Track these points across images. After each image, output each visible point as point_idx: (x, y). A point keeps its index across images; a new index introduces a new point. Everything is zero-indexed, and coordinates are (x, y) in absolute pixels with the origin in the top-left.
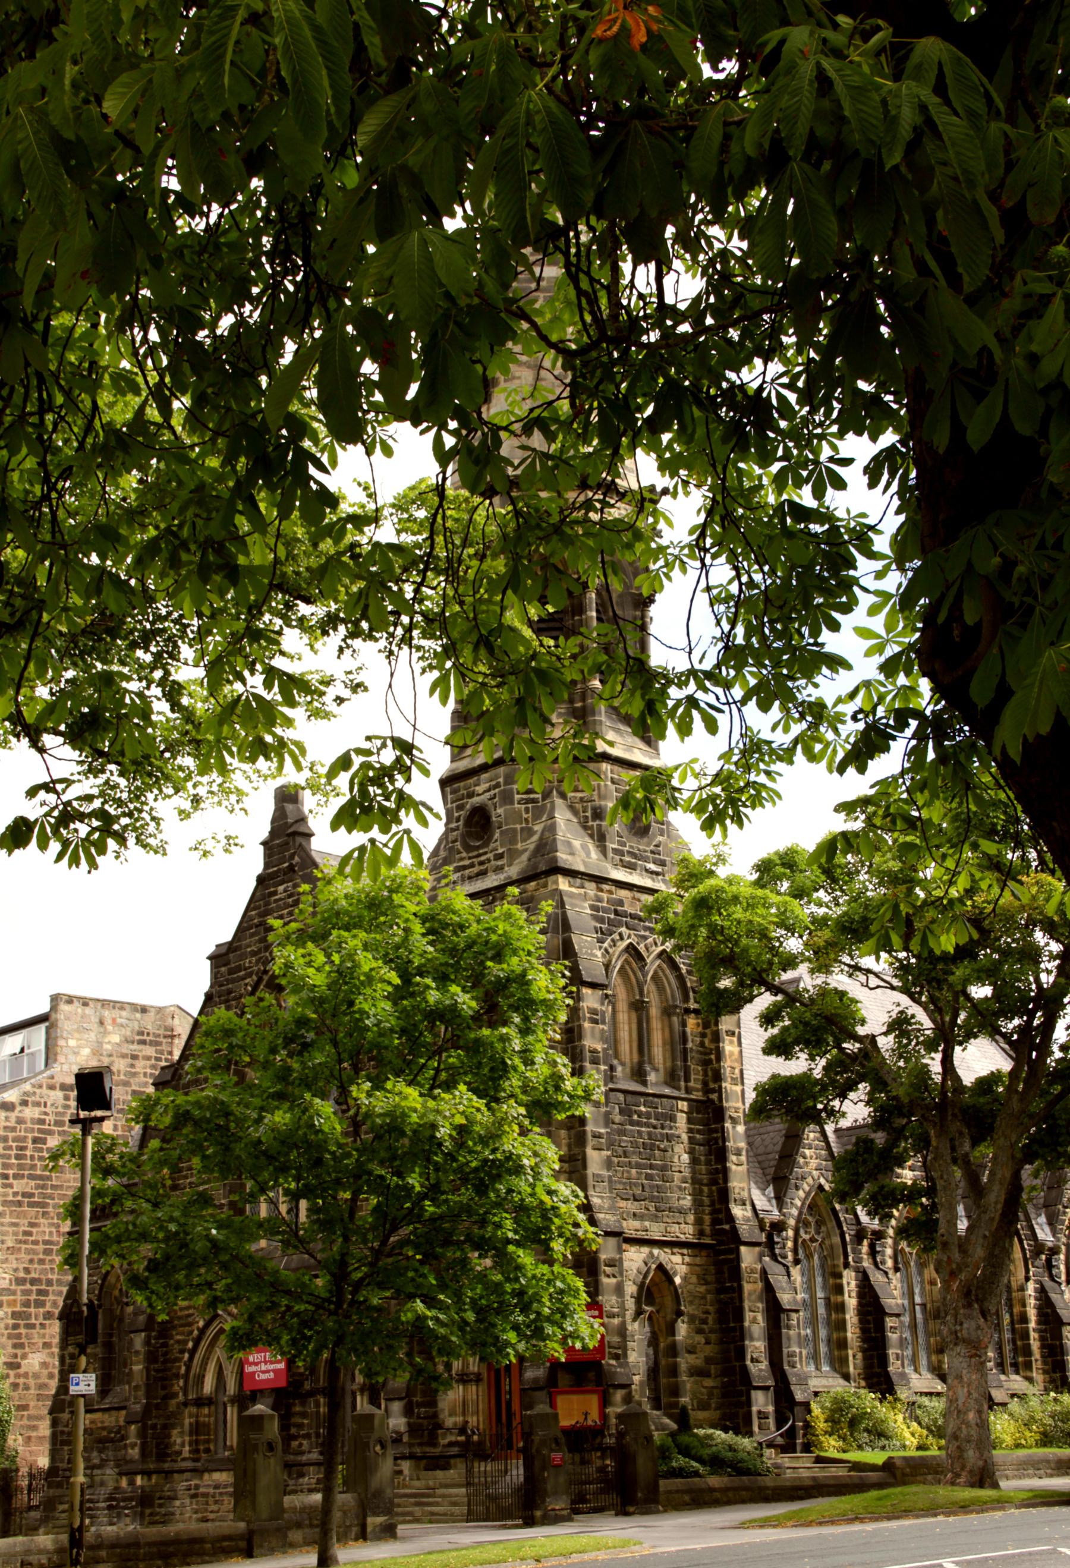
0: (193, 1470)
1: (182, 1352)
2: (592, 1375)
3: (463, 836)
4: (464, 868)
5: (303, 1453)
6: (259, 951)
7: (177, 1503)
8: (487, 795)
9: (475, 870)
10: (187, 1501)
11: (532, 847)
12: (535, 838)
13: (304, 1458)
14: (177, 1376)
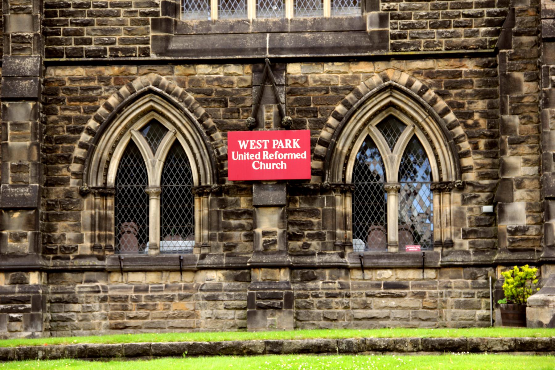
1: (80, 131)
5: (313, 254)
7: (77, 307)
10: (97, 305)
13: (317, 260)
14: (67, 159)
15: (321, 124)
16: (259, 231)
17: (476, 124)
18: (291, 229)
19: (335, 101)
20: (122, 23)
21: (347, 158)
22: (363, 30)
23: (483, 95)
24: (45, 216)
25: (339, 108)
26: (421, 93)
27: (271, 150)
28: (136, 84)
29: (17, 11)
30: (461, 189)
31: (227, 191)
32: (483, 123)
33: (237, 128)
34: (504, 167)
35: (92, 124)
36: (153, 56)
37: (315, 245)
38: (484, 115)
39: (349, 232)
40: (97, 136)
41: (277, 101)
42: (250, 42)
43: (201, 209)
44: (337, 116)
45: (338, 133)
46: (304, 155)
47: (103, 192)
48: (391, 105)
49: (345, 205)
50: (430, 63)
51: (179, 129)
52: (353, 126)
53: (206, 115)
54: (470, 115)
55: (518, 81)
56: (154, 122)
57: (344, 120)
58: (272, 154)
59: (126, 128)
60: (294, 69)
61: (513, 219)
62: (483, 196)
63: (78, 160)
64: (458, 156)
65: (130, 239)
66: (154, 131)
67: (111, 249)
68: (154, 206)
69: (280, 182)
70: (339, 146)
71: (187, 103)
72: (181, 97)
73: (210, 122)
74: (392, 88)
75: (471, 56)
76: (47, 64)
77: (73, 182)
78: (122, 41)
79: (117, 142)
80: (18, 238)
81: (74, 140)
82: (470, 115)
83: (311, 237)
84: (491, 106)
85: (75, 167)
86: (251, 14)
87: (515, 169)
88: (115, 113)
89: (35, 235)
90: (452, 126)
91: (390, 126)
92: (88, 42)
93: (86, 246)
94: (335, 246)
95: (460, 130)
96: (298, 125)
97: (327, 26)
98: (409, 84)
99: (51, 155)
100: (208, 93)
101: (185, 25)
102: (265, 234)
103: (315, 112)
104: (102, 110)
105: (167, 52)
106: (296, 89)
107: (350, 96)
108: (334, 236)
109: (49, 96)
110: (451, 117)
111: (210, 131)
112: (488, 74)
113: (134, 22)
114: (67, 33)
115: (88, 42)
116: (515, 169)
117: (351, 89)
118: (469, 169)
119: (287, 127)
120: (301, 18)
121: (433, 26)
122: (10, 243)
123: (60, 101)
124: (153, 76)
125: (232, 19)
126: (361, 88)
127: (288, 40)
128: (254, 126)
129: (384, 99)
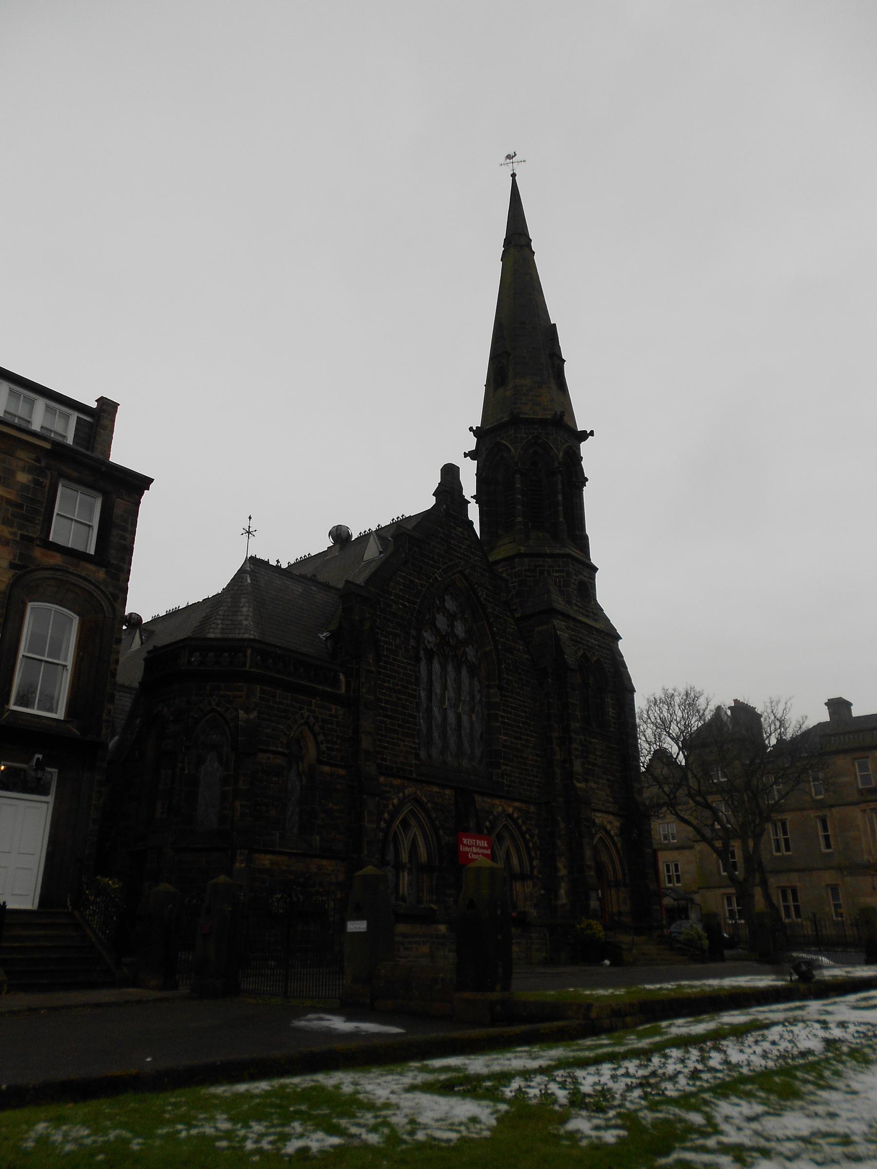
64: (531, 860)
104: (391, 807)
110: (527, 836)
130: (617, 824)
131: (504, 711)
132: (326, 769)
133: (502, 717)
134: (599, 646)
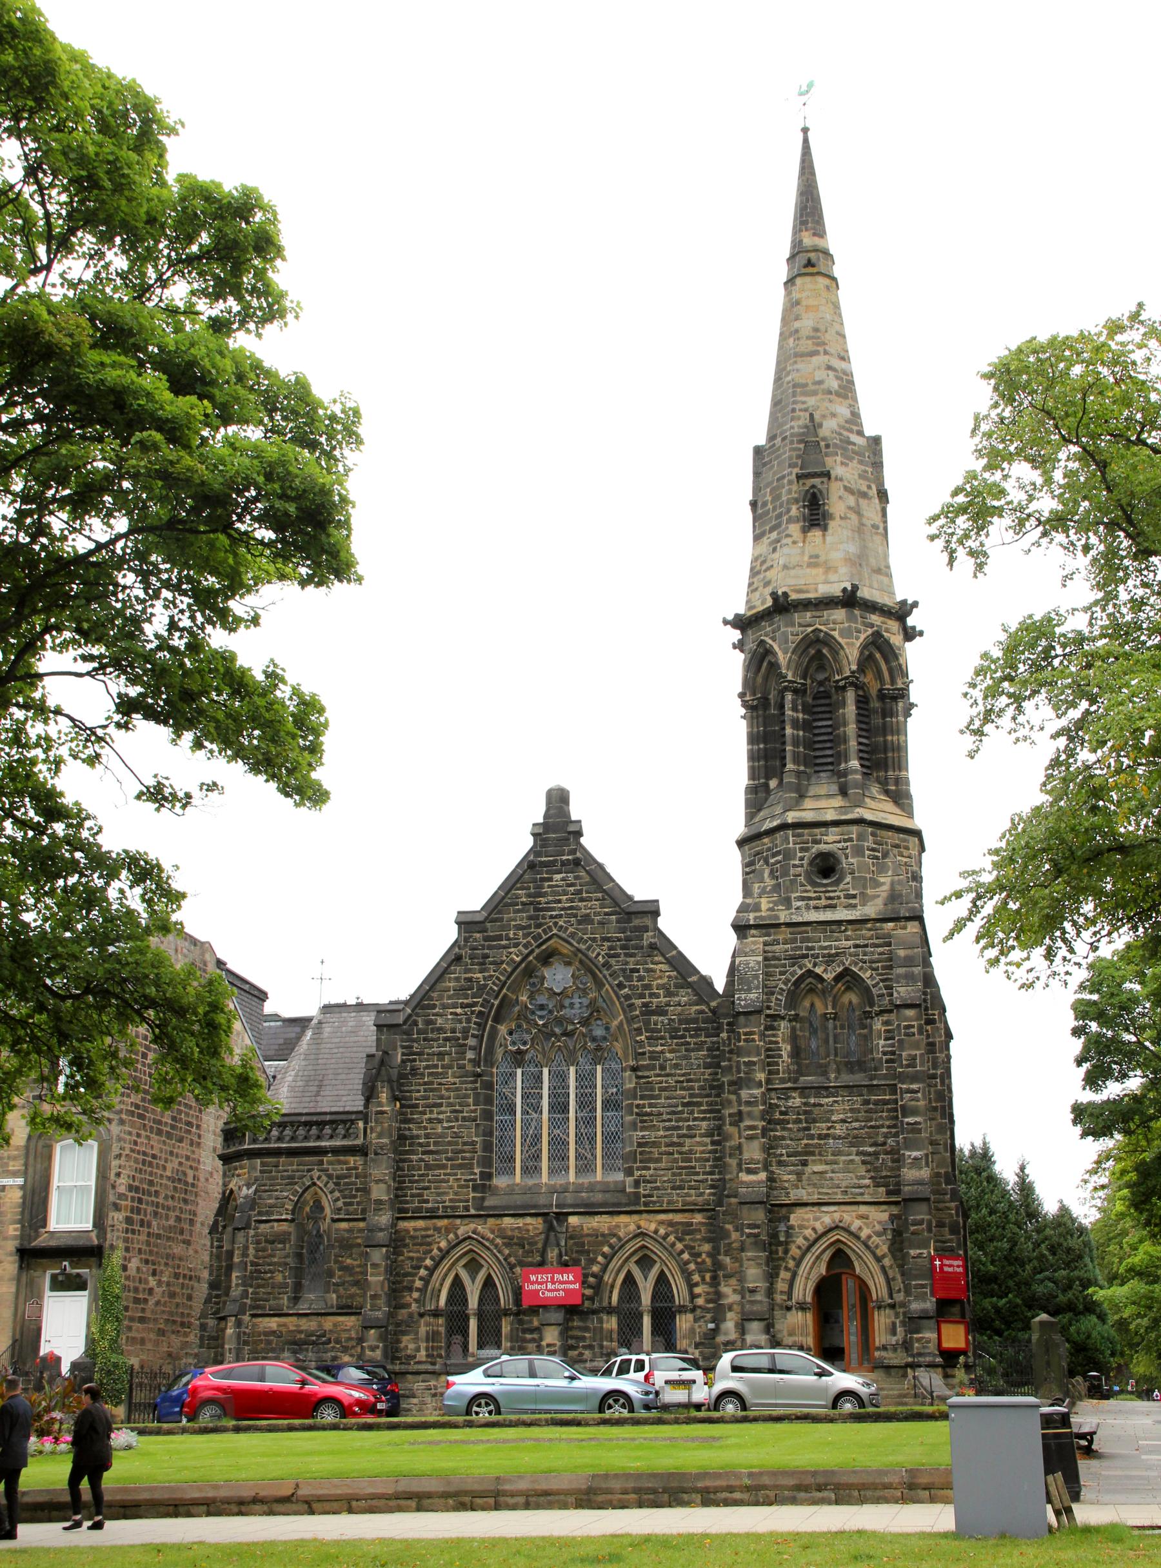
0: (433, 1373)
1: (419, 1268)
2: (956, 1309)
3: (806, 872)
4: (810, 899)
6: (529, 926)
7: (415, 1401)
8: (840, 845)
9: (823, 902)
10: (429, 1399)
11: (884, 895)
12: (886, 888)
15: (593, 1261)
16: (544, 1343)
17: (704, 1262)
18: (570, 1342)
19: (602, 1244)
20: (451, 1187)
21: (612, 1286)
22: (623, 1191)
23: (708, 1240)
24: (392, 1332)
25: (606, 1249)
26: (665, 1238)
27: (553, 1282)
28: (460, 1232)
29: (377, 1182)
30: (693, 1310)
31: (525, 1313)
32: (708, 1261)
33: (531, 1264)
34: (719, 1295)
35: (428, 1262)
36: (473, 1212)
37: (587, 1354)
38: (709, 1254)
39: (615, 1344)
40: (431, 1271)
41: (558, 1245)
42: (542, 1200)
43: (506, 1327)
44: (604, 1255)
45: (604, 1269)
46: (577, 1286)
47: (436, 1314)
48: (644, 1247)
49: (611, 1323)
50: (670, 1216)
51: (491, 1266)
52: (615, 1264)
53: (510, 1255)
54: (699, 1255)
55: (728, 1231)
56: (473, 1259)
57: (609, 1258)
58: (553, 1285)
59: (453, 1264)
60: (573, 1220)
61: (726, 1334)
62: (709, 1316)
63: (418, 1290)
64: (691, 1286)
65: (457, 1349)
66: (473, 1266)
67: (440, 1356)
68: (473, 1324)
69: (560, 1307)
70: (606, 1278)
71: (496, 1246)
72: (492, 1241)
73: (512, 1260)
74: (643, 1235)
75: (700, 1211)
76: (398, 1219)
77: (414, 1306)
78: (451, 1200)
79: (446, 1275)
80: (373, 1349)
81: (415, 1275)
82: (699, 1255)
83: (584, 1347)
84: (714, 1248)
85: (416, 1295)
86: (545, 1178)
87: (727, 1296)
88: (445, 1254)
89: (385, 1347)
90: (687, 1263)
91: (645, 1262)
92: (427, 1201)
93: (422, 1355)
94: (602, 1355)
95: (692, 1266)
96: (576, 1262)
97: (598, 1187)
98: (656, 1232)
99: (397, 1289)
100: (511, 1238)
101: (496, 1187)
102: (549, 1345)
103: (588, 1252)
105: (482, 1208)
106: (575, 1236)
107: (613, 1240)
108: (601, 1347)
109: (397, 1243)
110: (686, 1256)
111: (512, 1267)
112: (711, 1224)
113: (460, 1187)
114: (412, 1196)
115: (427, 1201)
116: (727, 1296)
117: (615, 1235)
118: (699, 1296)
119: (566, 1265)
120: (580, 1181)
121: (673, 1188)
122: (368, 1353)
123: (406, 1246)
124: (472, 1226)
125: (531, 1182)
126: (621, 1234)
127: (569, 1198)
128: (542, 1263)
129: (638, 1243)
130: (885, 1216)
131: (642, 1098)
132: (344, 1225)
133: (638, 1106)
134: (856, 946)
